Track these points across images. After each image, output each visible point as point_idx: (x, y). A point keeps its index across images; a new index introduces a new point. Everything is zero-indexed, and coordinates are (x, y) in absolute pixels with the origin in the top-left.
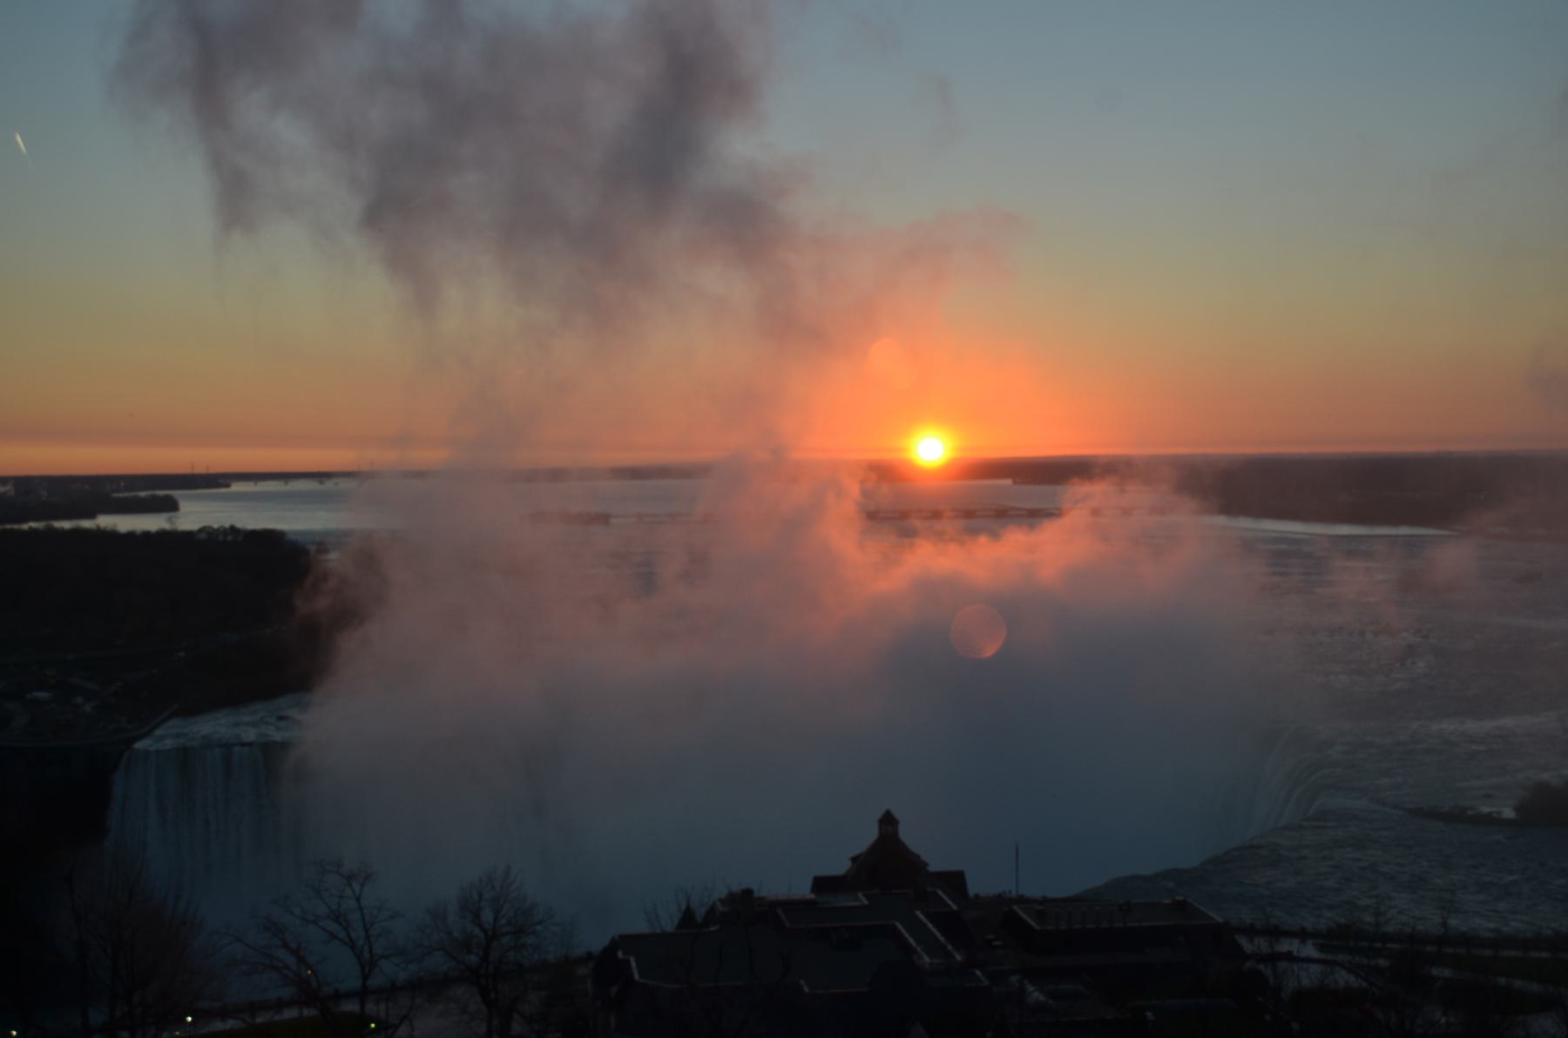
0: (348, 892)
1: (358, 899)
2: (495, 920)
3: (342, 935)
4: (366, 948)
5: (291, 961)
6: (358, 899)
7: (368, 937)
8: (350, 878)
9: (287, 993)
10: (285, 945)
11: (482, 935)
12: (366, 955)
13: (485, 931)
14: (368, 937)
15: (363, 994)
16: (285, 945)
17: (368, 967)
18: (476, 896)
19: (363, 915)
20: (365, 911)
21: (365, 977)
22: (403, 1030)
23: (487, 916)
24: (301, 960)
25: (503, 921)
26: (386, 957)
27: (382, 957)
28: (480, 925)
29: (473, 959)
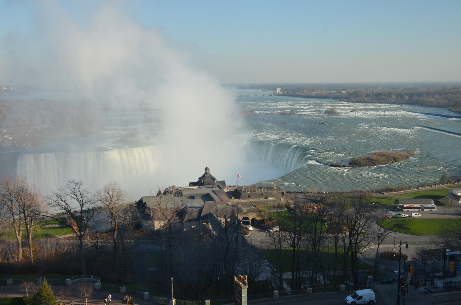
0: (76, 187)
1: (79, 189)
2: (113, 193)
3: (75, 197)
4: (81, 200)
5: (64, 204)
6: (79, 189)
7: (82, 198)
8: (76, 184)
9: (63, 211)
10: (62, 200)
11: (109, 197)
12: (82, 202)
13: (110, 197)
14: (82, 198)
15: (82, 212)
16: (62, 200)
17: (82, 205)
18: (108, 188)
19: (80, 193)
20: (81, 192)
21: (82, 207)
22: (92, 220)
23: (111, 193)
24: (66, 203)
25: (115, 194)
26: (86, 203)
27: (85, 203)
28: (109, 195)
29: (108, 203)
